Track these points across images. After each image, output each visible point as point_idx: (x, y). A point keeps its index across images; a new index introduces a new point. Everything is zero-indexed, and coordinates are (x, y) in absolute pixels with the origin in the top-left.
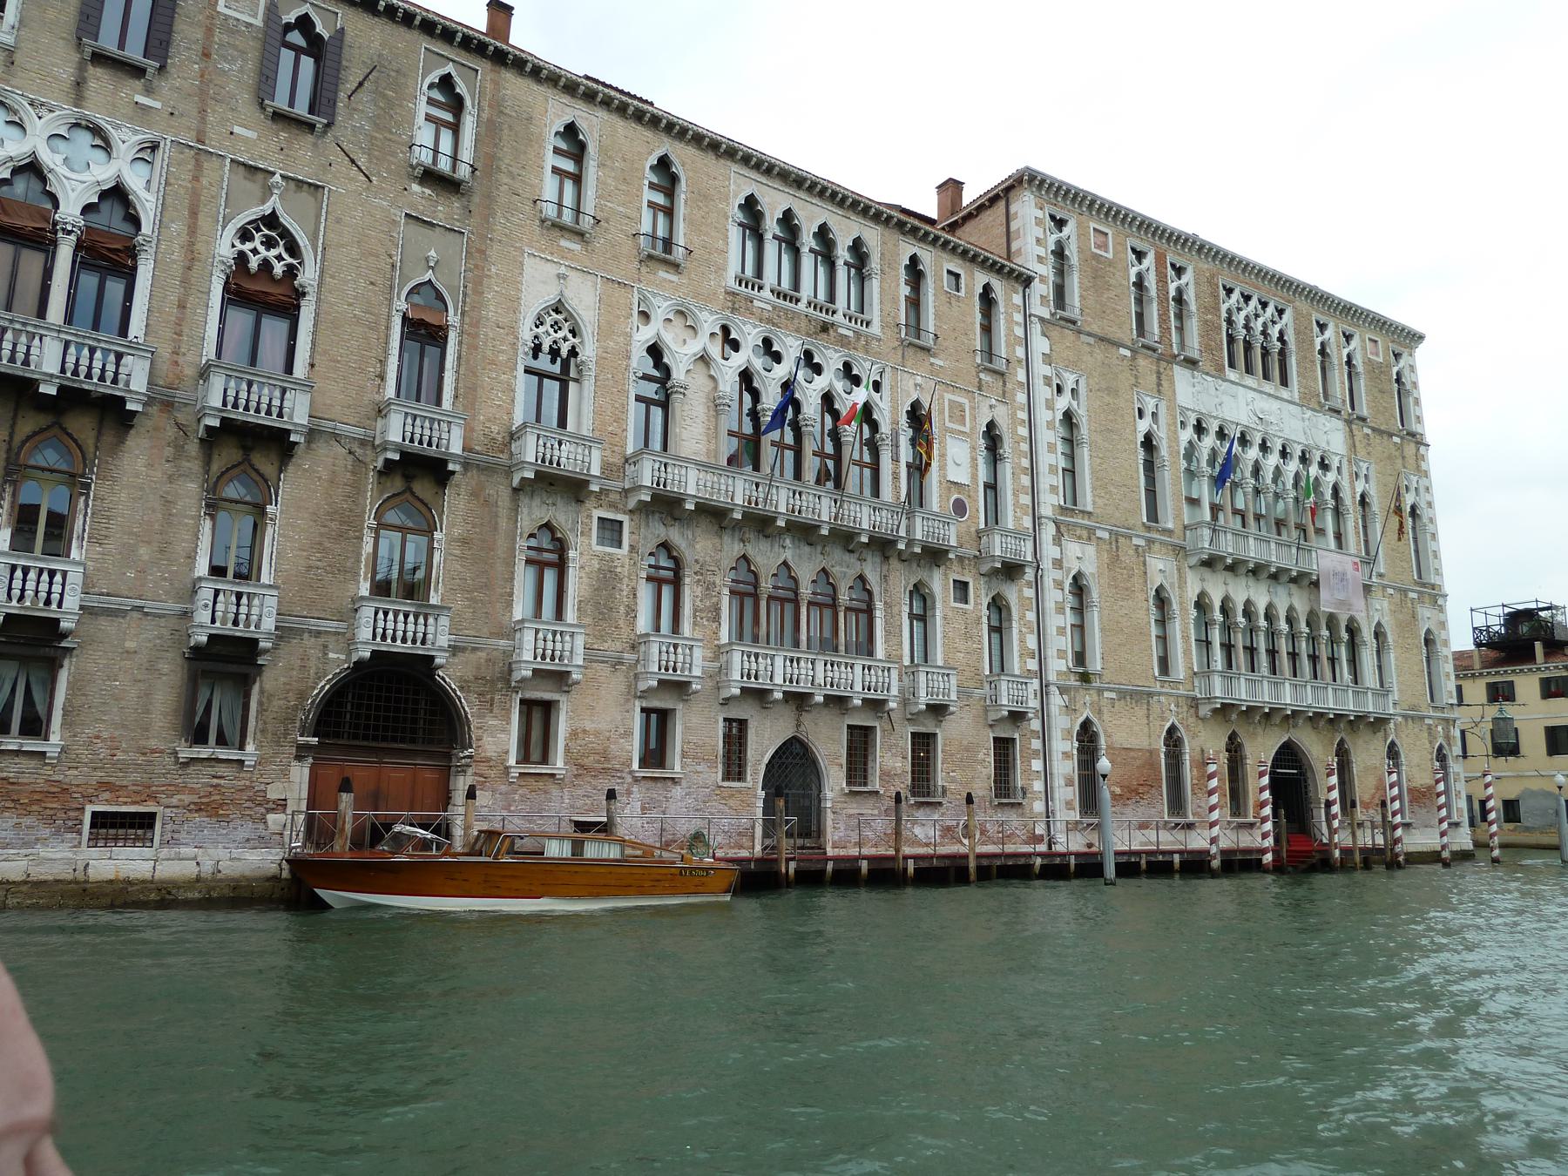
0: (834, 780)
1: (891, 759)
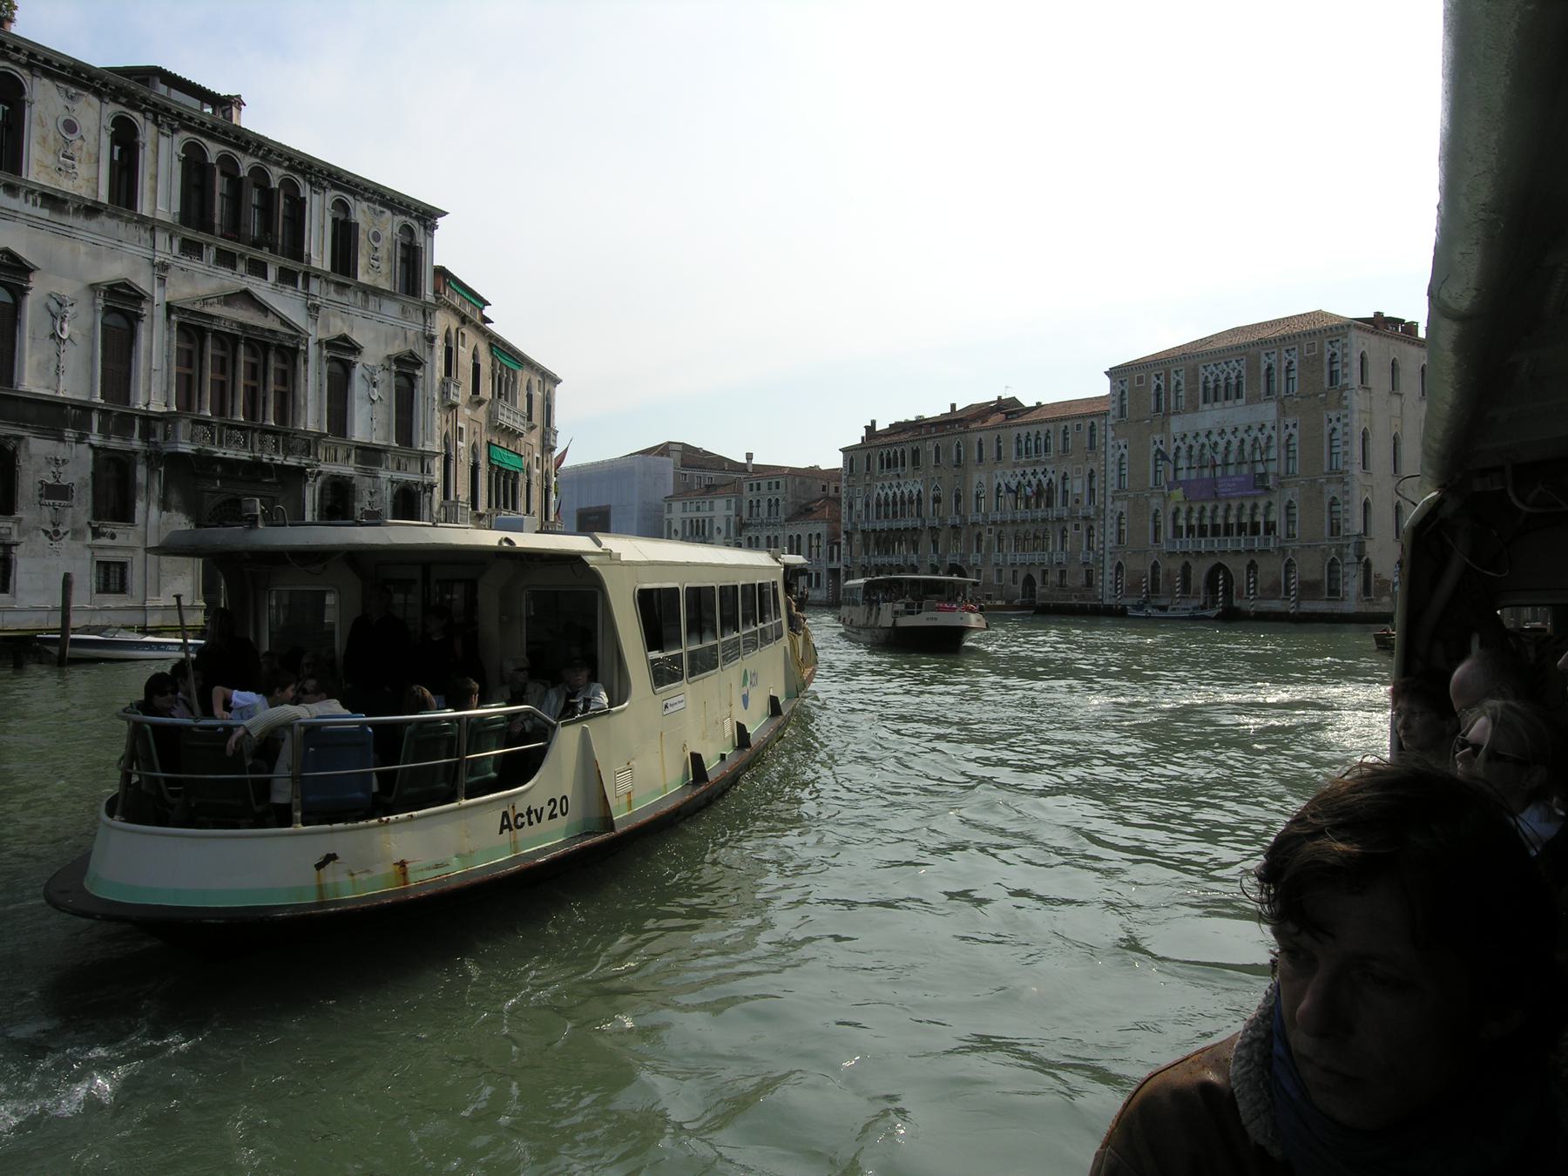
0: (1039, 584)
1: (1053, 577)
